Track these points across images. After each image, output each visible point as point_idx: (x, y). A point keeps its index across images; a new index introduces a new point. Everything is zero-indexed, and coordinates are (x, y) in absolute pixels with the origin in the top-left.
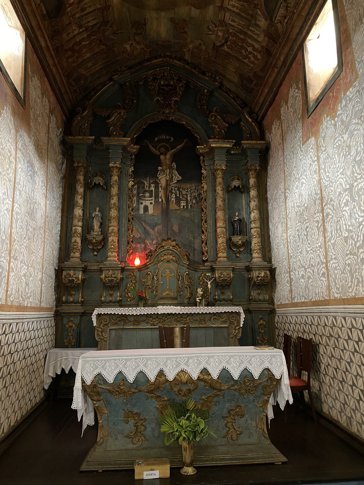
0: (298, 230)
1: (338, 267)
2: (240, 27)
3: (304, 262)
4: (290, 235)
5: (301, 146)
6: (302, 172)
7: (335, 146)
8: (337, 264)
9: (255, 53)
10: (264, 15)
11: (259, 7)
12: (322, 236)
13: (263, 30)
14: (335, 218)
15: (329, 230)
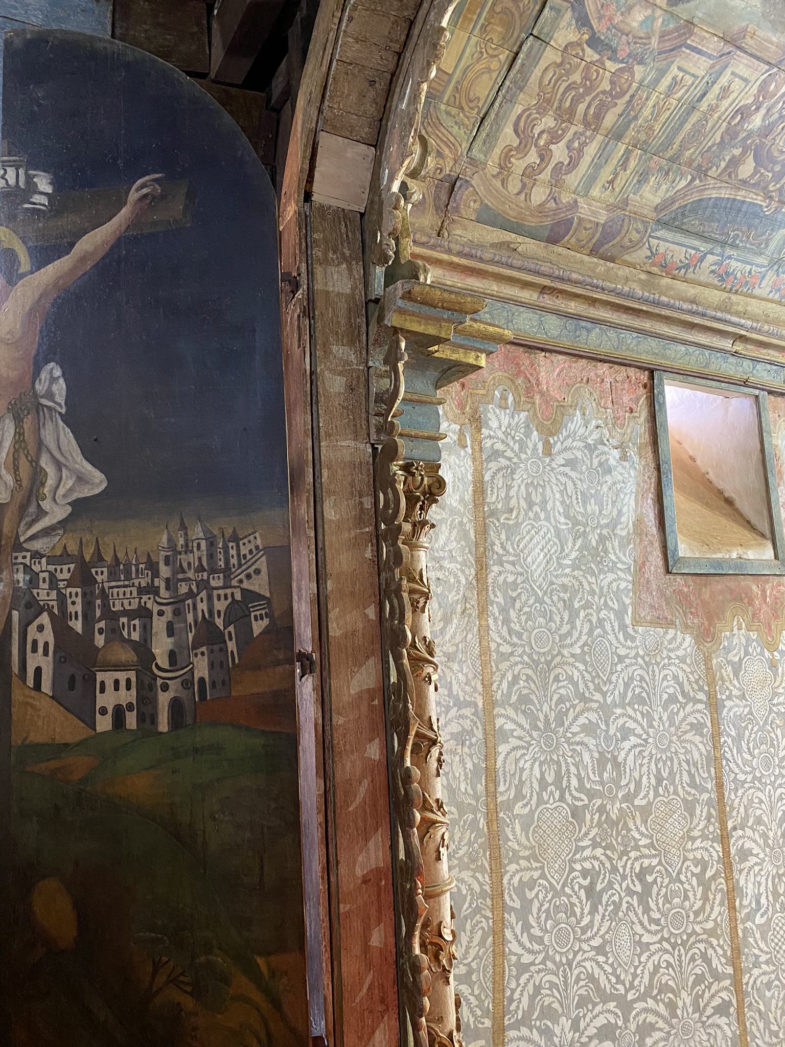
0: (585, 873)
1: (777, 983)
2: (647, 112)
3: (619, 980)
4: (532, 884)
5: (628, 621)
6: (623, 696)
7: (775, 709)
8: (773, 976)
9: (546, 175)
10: (673, 201)
11: (697, 181)
12: (721, 904)
13: (626, 202)
14: (768, 866)
15: (750, 890)
